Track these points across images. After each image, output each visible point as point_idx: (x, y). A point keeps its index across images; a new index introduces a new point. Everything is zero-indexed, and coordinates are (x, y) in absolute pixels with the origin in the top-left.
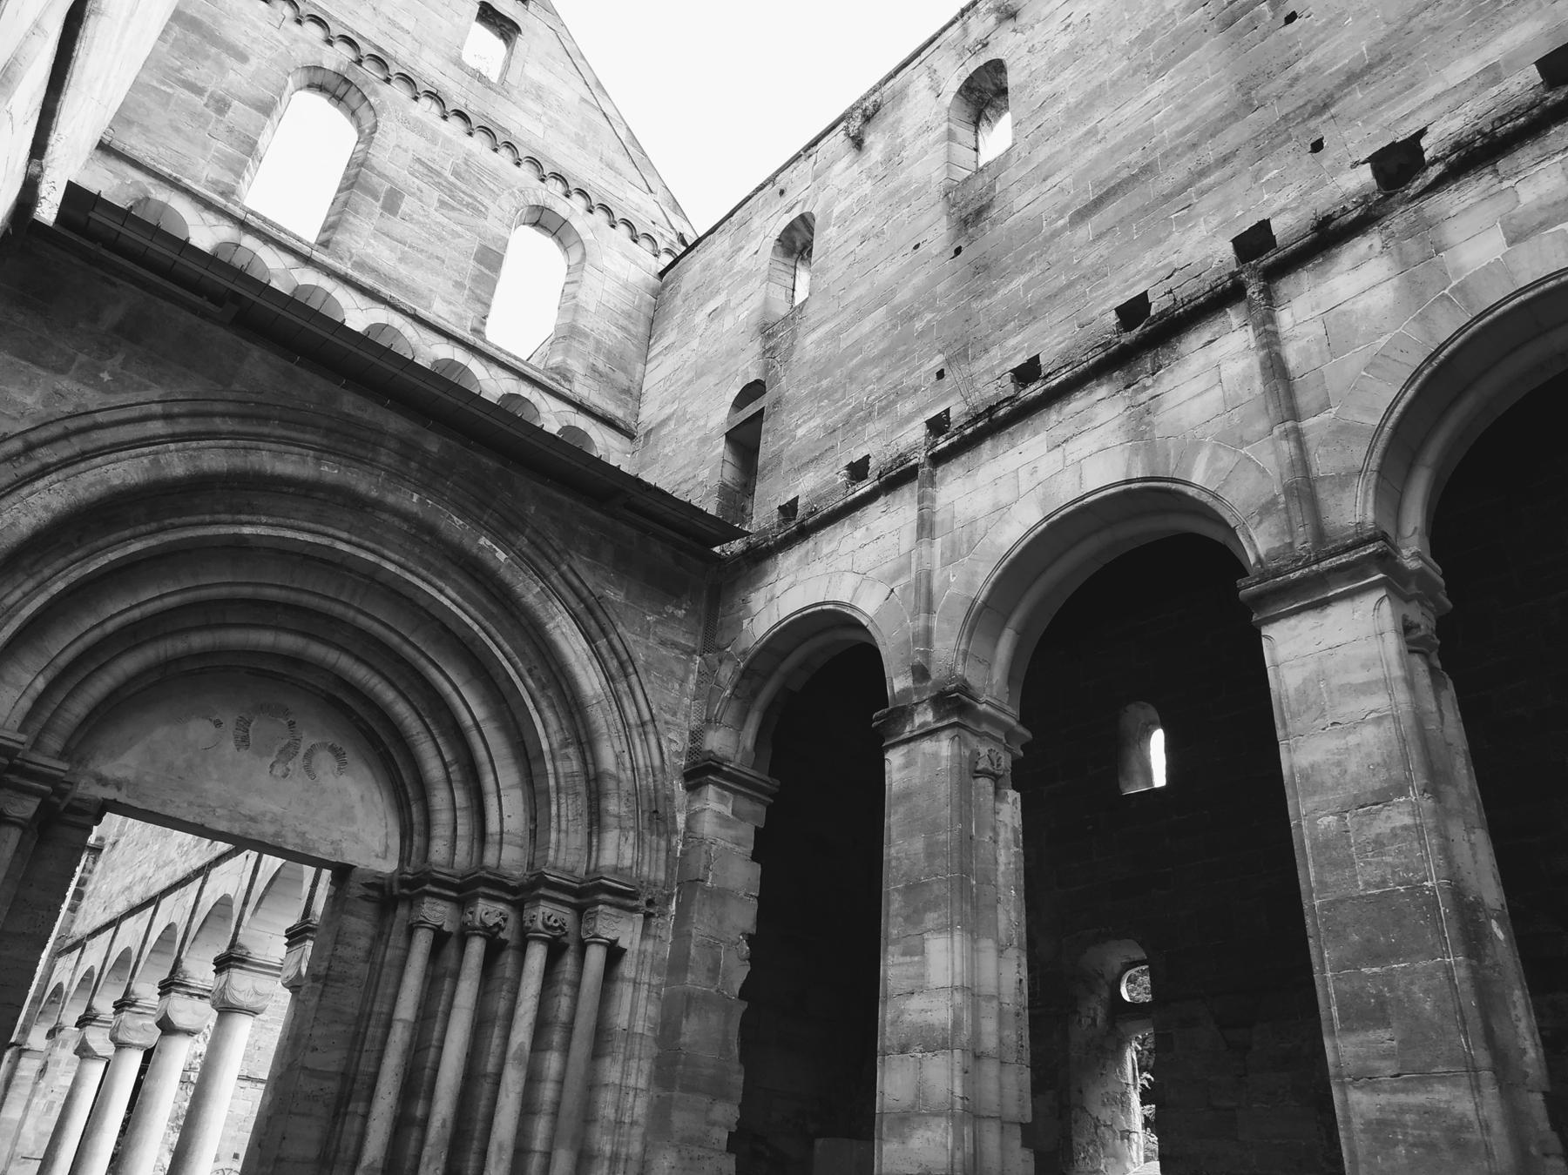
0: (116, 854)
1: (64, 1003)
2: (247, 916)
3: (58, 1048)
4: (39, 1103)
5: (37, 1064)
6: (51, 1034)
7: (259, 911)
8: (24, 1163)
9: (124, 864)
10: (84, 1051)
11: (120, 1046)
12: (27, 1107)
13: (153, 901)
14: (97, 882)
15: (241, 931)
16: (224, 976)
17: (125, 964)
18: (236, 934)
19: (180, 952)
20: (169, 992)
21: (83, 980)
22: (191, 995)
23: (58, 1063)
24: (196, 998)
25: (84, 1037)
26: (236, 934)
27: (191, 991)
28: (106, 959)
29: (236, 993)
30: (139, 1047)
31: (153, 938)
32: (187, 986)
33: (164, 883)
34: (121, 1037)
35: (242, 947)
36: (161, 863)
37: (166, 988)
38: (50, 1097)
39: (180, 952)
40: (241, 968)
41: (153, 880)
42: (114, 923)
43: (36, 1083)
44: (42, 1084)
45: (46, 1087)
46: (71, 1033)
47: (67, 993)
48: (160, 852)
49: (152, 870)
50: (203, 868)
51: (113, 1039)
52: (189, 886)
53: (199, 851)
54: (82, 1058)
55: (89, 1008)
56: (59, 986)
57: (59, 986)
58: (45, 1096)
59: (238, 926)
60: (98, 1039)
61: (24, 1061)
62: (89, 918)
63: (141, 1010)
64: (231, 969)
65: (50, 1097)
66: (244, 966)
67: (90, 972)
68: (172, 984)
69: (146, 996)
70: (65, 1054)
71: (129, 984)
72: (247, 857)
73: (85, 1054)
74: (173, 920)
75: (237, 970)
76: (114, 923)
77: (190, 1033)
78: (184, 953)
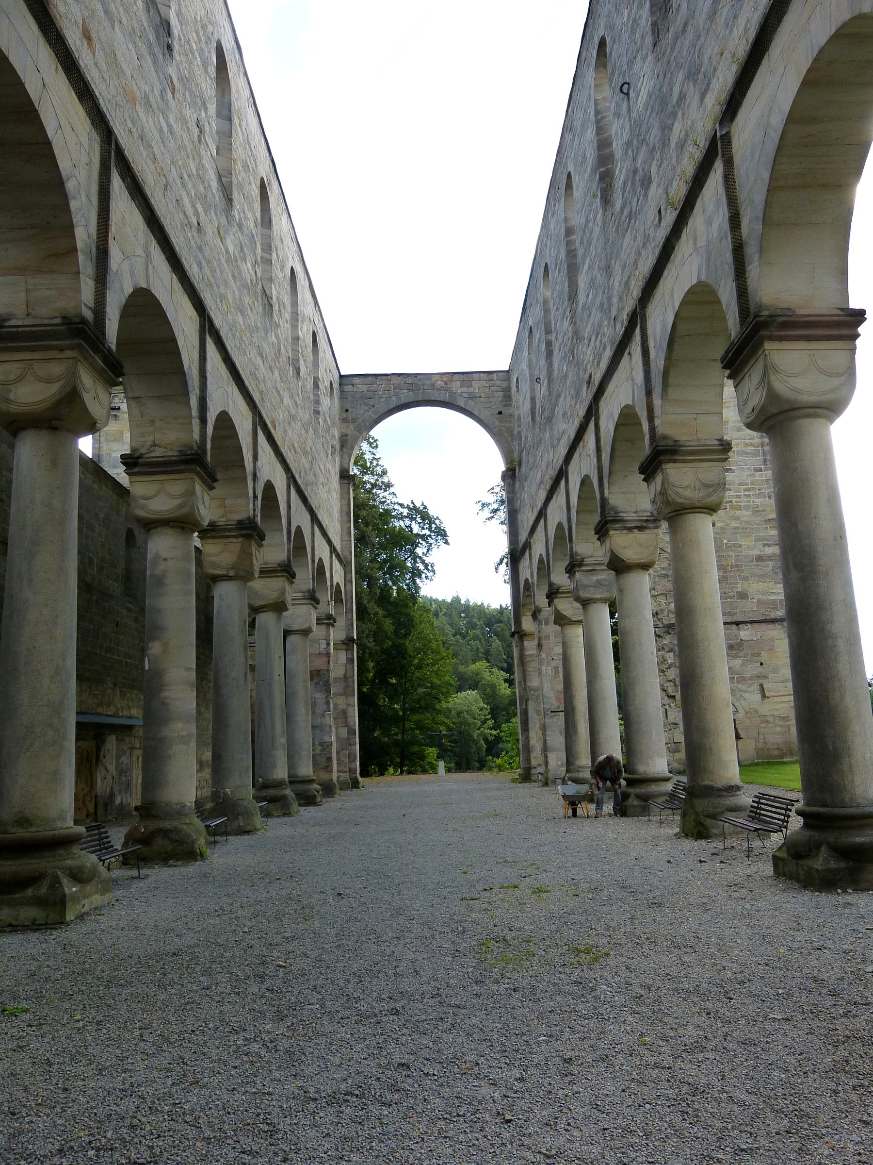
0: (523, 468)
1: (534, 592)
2: (657, 402)
3: (544, 626)
4: (547, 670)
5: (535, 642)
6: (535, 616)
7: (670, 390)
8: (554, 716)
9: (531, 469)
10: (561, 620)
11: (585, 603)
12: (540, 674)
13: (562, 474)
14: (521, 496)
15: (657, 422)
16: (659, 479)
17: (563, 536)
18: (652, 429)
19: (602, 493)
20: (607, 531)
21: (538, 568)
22: (630, 529)
23: (548, 637)
24: (636, 531)
25: (556, 608)
26: (652, 429)
27: (629, 525)
28: (547, 542)
29: (680, 491)
30: (604, 600)
31: (574, 500)
32: (621, 521)
33: (563, 451)
34: (583, 594)
35: (665, 437)
36: (556, 442)
37: (602, 531)
38: (554, 664)
39: (602, 493)
40: (675, 461)
41: (555, 460)
42: (542, 514)
43: (539, 655)
44: (543, 655)
45: (547, 658)
46: (547, 612)
47: (533, 583)
48: (551, 437)
49: (551, 454)
50: (590, 408)
51: (578, 599)
52: (586, 437)
53: (582, 402)
54: (561, 626)
55: (551, 585)
56: (527, 580)
57: (527, 580)
58: (549, 664)
59: (651, 418)
60: (567, 607)
61: (526, 643)
62: (525, 523)
63: (590, 568)
64: (663, 466)
65: (554, 664)
66: (677, 457)
67: (541, 561)
68: (607, 522)
69: (590, 554)
70: (552, 629)
71: (571, 548)
72: (629, 353)
73: (562, 622)
74: (584, 473)
75: (670, 465)
76: (542, 514)
77: (645, 567)
78: (606, 491)
